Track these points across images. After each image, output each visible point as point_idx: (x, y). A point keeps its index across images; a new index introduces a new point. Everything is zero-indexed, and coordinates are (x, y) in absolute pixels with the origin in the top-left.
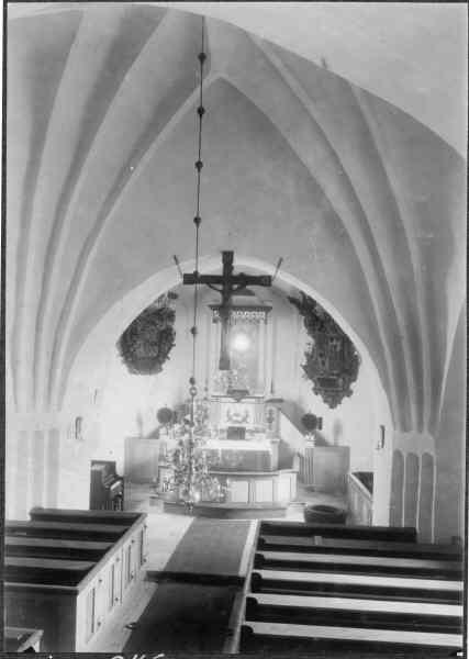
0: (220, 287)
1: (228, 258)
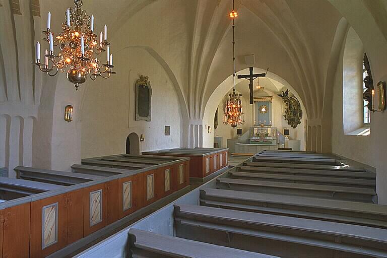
0: (249, 78)
1: (251, 69)
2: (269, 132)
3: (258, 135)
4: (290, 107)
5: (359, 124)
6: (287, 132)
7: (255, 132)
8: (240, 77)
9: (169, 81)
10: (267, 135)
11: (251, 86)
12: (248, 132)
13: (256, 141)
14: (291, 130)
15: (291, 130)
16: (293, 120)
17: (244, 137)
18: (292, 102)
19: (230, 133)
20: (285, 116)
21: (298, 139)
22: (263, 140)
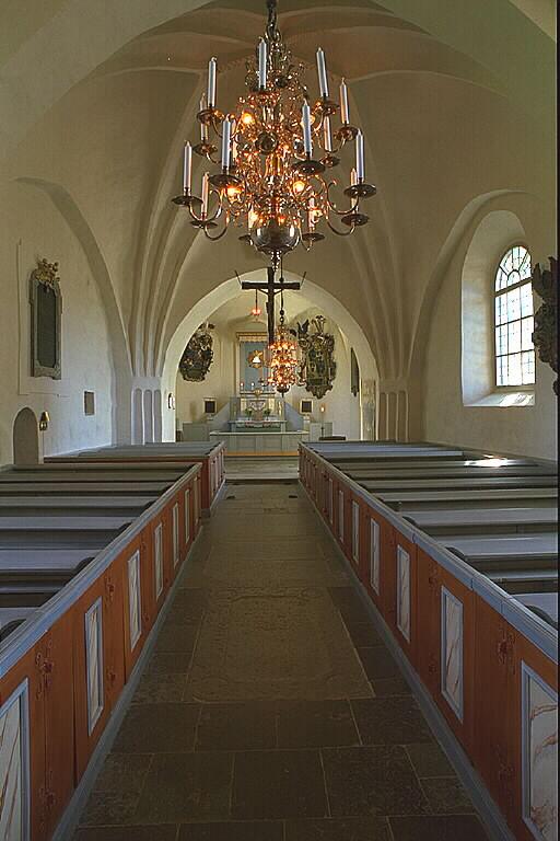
0: (267, 291)
2: (272, 406)
3: (249, 413)
4: (312, 355)
5: (488, 387)
6: (307, 407)
7: (243, 407)
8: (246, 286)
9: (91, 281)
10: (268, 413)
12: (227, 408)
14: (314, 402)
15: (314, 402)
16: (319, 382)
17: (220, 418)
18: (316, 345)
19: (188, 411)
22: (260, 425)
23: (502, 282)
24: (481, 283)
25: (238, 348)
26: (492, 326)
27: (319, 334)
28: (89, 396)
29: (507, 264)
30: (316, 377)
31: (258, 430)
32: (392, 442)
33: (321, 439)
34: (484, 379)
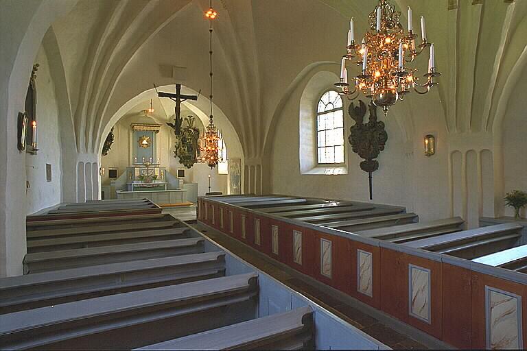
0: (175, 99)
1: (178, 88)
2: (157, 173)
4: (184, 140)
6: (181, 173)
7: (137, 173)
8: (161, 95)
9: (51, 80)
10: (155, 178)
11: (178, 109)
13: (141, 187)
14: (186, 170)
15: (186, 170)
17: (119, 181)
20: (176, 152)
21: (195, 181)
22: (148, 184)
23: (321, 108)
24: (310, 108)
25: (131, 134)
26: (316, 131)
27: (190, 127)
28: (48, 166)
29: (325, 98)
30: (187, 154)
31: (149, 189)
32: (252, 195)
33: (207, 194)
34: (311, 160)
